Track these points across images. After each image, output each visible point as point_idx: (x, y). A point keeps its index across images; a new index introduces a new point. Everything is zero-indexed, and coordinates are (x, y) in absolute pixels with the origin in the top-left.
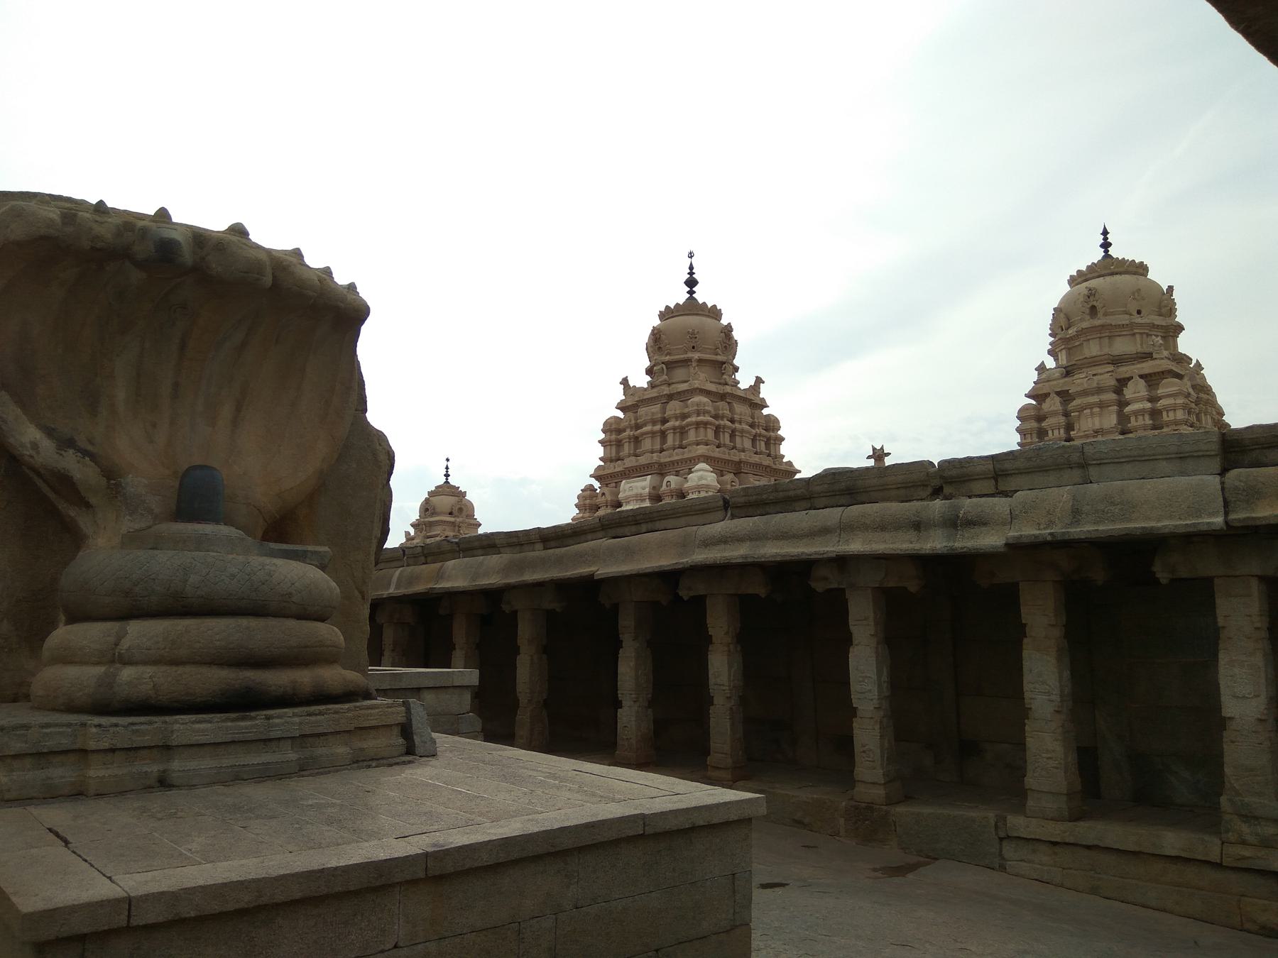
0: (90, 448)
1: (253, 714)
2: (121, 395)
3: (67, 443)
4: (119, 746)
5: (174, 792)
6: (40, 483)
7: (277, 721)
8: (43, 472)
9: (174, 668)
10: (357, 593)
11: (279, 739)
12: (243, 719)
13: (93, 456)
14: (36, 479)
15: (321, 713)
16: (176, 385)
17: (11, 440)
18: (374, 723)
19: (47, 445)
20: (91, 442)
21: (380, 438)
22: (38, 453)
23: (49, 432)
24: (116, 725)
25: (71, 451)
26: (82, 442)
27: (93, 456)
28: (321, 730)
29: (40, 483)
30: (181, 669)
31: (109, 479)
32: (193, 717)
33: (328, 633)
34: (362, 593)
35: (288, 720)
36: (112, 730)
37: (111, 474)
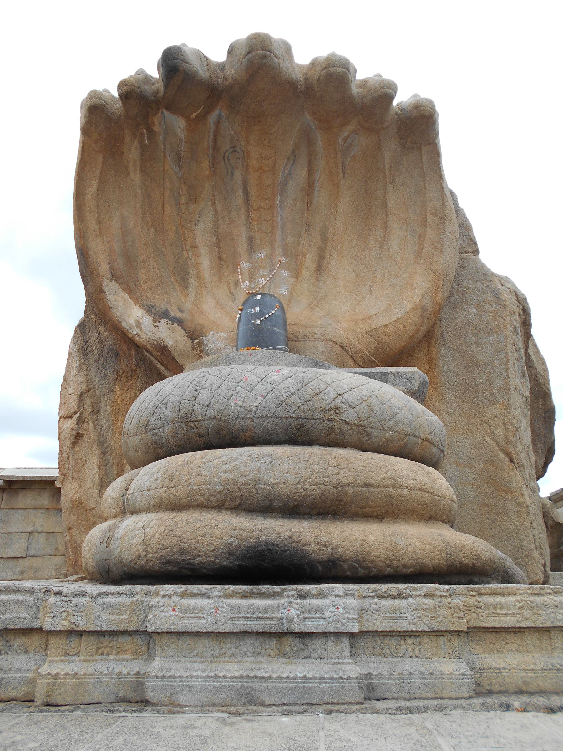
0: (179, 315)
1: (277, 589)
2: (205, 261)
3: (160, 315)
4: (83, 627)
5: (148, 715)
6: (159, 366)
7: (316, 602)
8: (149, 347)
9: (173, 514)
10: (501, 455)
11: (326, 635)
12: (262, 595)
13: (180, 322)
14: (156, 362)
15: (400, 596)
16: (251, 239)
17: (124, 325)
18: (509, 622)
19: (147, 320)
20: (180, 310)
21: (504, 281)
22: (141, 330)
23: (149, 309)
24: (107, 594)
25: (162, 321)
26: (174, 312)
27: (180, 322)
28: (404, 625)
29: (159, 366)
30: (184, 516)
31: (193, 339)
32: (181, 588)
33: (437, 481)
34: (508, 455)
35: (335, 605)
36: (75, 600)
37: (195, 335)
